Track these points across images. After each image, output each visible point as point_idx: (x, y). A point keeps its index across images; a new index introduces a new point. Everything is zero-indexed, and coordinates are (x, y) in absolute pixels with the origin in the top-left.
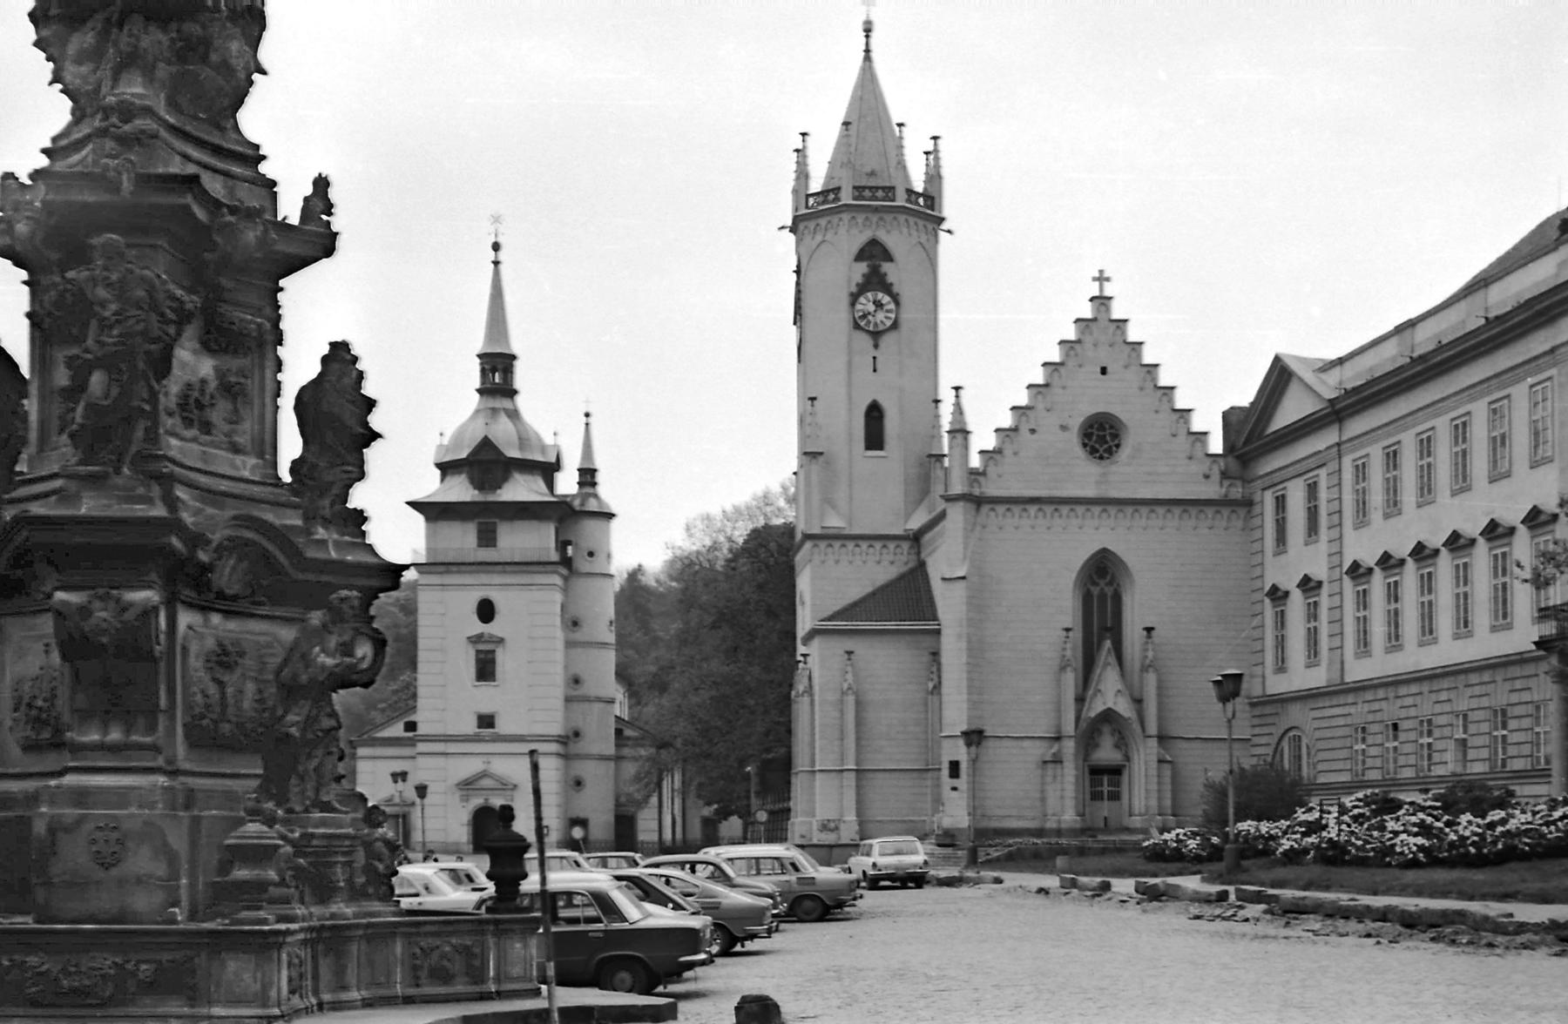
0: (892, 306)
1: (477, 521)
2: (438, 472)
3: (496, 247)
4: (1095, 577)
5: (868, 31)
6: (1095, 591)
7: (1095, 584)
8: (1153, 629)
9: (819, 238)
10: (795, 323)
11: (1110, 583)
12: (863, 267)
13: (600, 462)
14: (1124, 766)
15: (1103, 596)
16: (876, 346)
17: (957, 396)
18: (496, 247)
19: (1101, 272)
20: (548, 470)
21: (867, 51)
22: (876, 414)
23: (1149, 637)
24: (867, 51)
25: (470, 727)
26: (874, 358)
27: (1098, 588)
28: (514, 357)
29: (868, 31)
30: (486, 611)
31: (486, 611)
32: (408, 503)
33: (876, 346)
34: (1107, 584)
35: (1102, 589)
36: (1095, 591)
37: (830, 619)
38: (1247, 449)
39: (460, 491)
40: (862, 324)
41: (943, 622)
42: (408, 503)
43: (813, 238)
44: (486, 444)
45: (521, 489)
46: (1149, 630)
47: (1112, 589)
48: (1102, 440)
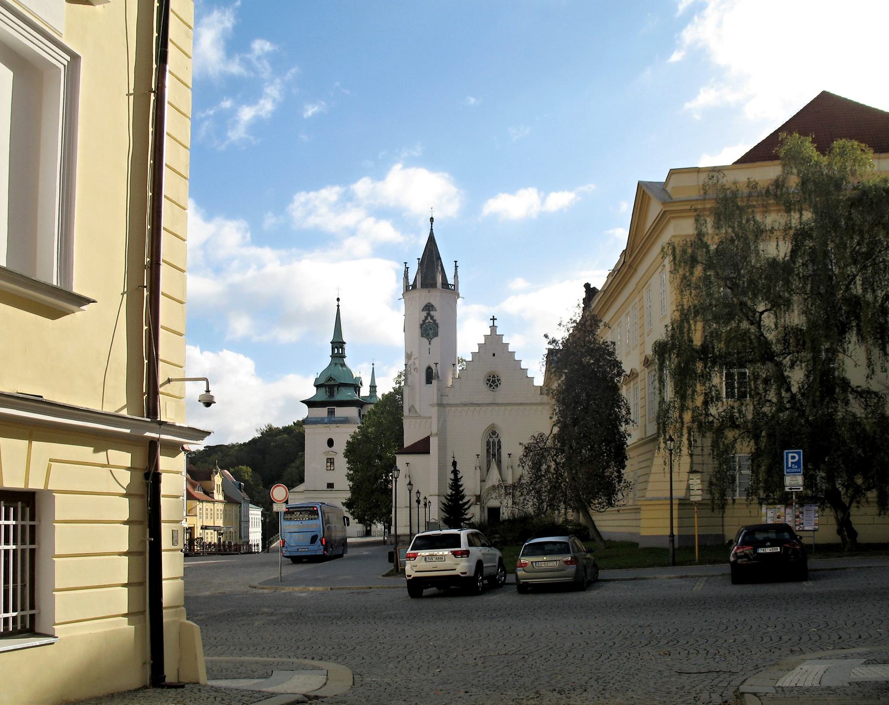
1: (327, 408)
2: (315, 388)
3: (338, 300)
6: (491, 440)
7: (491, 437)
12: (425, 314)
13: (377, 383)
15: (494, 443)
16: (430, 344)
18: (338, 300)
20: (356, 387)
22: (429, 370)
25: (325, 488)
27: (492, 439)
28: (345, 343)
30: (330, 443)
31: (330, 443)
32: (301, 401)
33: (430, 344)
36: (491, 440)
39: (324, 397)
42: (301, 401)
44: (330, 379)
45: (346, 394)
47: (498, 439)
48: (494, 382)
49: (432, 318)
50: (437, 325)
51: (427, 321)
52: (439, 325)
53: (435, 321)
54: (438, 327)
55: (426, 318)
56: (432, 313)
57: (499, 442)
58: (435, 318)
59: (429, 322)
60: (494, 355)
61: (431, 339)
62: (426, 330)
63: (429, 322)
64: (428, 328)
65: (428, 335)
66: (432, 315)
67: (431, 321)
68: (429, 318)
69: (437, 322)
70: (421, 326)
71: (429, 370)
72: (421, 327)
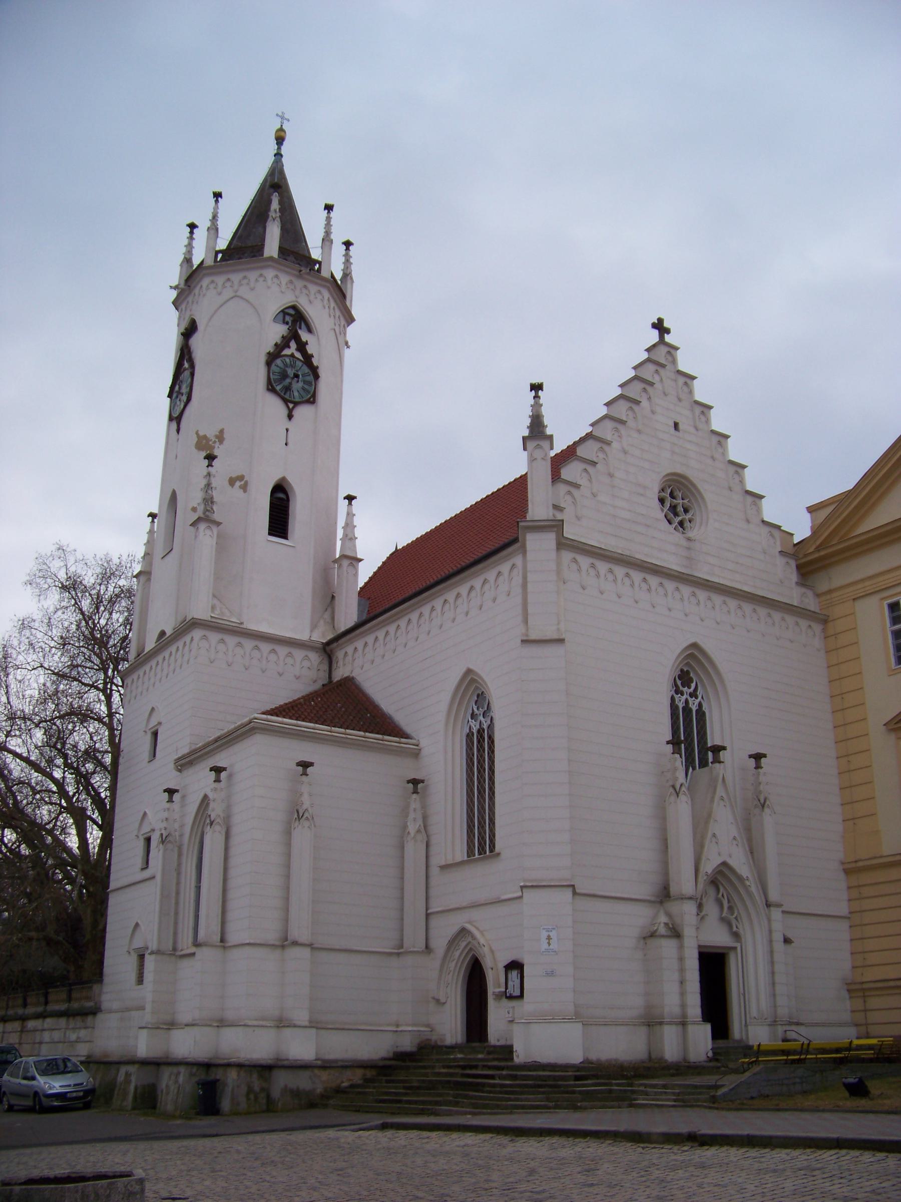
0: (311, 378)
4: (679, 683)
5: (280, 140)
8: (765, 756)
9: (228, 293)
10: (170, 396)
11: (694, 695)
14: (735, 948)
15: (687, 709)
16: (290, 417)
17: (536, 397)
19: (660, 321)
21: (278, 155)
23: (758, 767)
24: (278, 155)
26: (287, 430)
29: (280, 140)
33: (290, 417)
34: (691, 695)
35: (687, 701)
37: (273, 712)
38: (822, 553)
40: (278, 388)
41: (423, 743)
43: (220, 294)
46: (758, 757)
47: (697, 702)
49: (302, 347)
50: (315, 372)
51: (287, 352)
52: (322, 372)
53: (308, 359)
54: (317, 377)
55: (284, 343)
56: (304, 336)
57: (701, 714)
58: (310, 349)
59: (292, 355)
60: (676, 426)
61: (296, 404)
62: (284, 375)
63: (292, 355)
64: (291, 372)
65: (288, 389)
66: (304, 340)
67: (298, 355)
68: (293, 345)
69: (315, 362)
70: (272, 358)
71: (281, 495)
72: (269, 364)
